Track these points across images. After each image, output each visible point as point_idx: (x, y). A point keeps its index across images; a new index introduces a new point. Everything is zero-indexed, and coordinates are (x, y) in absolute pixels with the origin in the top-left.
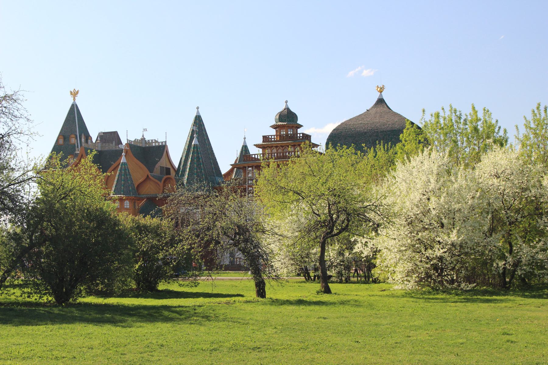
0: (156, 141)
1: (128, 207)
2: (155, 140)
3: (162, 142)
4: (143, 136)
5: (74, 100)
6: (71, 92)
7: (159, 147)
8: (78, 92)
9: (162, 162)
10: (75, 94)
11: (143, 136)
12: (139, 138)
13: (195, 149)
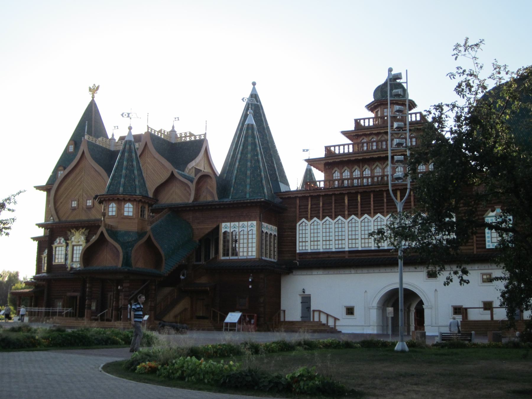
0: (191, 135)
1: (131, 214)
2: (190, 133)
3: (200, 135)
4: (173, 127)
5: (93, 97)
6: (90, 89)
7: (195, 141)
8: (98, 88)
9: (198, 163)
10: (94, 90)
11: (173, 127)
12: (168, 129)
13: (250, 131)
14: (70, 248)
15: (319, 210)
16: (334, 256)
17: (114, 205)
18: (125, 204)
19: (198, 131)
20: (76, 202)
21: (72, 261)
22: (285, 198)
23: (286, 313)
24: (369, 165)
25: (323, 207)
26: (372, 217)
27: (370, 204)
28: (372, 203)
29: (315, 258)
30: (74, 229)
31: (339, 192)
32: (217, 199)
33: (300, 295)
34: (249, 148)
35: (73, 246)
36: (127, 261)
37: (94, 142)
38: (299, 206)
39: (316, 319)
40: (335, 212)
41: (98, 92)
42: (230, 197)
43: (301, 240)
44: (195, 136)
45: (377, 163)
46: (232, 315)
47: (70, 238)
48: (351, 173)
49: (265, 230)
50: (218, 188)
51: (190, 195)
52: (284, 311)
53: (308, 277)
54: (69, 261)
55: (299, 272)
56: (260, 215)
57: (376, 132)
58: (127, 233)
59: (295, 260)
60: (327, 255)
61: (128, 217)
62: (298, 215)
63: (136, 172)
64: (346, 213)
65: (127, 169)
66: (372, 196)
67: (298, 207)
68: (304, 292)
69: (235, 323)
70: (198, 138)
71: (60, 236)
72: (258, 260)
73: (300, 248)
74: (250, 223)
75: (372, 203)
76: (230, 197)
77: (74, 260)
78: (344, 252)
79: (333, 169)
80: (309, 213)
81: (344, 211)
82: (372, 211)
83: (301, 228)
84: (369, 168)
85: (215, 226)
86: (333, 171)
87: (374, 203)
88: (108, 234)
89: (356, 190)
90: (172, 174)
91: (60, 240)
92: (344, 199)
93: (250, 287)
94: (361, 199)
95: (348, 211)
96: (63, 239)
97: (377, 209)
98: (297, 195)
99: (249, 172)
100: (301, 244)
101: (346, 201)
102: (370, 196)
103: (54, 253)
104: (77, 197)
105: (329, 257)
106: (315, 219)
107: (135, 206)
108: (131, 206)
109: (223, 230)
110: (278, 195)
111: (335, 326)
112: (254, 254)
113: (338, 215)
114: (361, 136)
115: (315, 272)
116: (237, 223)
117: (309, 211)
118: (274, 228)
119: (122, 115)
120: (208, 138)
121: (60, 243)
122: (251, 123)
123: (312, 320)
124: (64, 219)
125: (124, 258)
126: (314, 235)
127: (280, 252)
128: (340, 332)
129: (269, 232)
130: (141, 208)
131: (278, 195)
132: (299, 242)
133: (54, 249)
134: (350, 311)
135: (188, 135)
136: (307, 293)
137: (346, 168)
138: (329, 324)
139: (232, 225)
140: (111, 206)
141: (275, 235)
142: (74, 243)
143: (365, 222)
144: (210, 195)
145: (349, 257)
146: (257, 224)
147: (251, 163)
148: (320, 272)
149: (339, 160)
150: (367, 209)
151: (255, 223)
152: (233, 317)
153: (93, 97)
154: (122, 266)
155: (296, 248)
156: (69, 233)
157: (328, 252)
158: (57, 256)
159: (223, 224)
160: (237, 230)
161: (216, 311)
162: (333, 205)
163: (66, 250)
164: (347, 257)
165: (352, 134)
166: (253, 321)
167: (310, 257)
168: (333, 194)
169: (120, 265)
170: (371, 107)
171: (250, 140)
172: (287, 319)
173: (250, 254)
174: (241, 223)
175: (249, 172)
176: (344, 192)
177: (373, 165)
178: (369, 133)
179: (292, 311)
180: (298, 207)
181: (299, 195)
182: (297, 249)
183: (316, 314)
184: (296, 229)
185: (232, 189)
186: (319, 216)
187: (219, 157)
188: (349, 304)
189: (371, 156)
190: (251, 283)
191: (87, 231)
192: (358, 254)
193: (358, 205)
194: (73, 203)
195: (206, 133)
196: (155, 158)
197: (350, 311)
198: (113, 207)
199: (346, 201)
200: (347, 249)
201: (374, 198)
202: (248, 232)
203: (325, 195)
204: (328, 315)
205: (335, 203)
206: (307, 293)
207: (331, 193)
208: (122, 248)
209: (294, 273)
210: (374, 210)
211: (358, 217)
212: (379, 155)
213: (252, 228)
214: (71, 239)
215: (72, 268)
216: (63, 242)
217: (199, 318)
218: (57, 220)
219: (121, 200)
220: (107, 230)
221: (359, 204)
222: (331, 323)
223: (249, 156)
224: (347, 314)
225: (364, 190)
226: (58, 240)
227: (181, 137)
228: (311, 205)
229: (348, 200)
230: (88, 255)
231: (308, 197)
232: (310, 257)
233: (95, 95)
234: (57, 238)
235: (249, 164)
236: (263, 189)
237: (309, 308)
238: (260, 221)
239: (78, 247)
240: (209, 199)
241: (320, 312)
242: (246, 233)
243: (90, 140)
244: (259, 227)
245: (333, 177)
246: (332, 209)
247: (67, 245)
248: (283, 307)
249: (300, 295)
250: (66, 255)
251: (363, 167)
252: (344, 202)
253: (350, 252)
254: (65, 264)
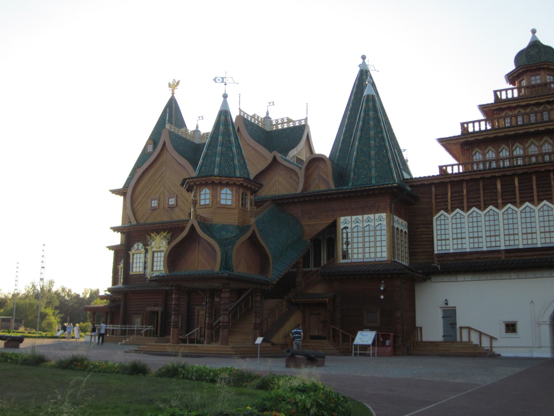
0: (289, 121)
1: (229, 202)
2: (288, 119)
3: (300, 121)
5: (173, 94)
7: (295, 128)
9: (298, 152)
10: (174, 85)
12: (263, 115)
13: (371, 104)
14: (149, 255)
15: (463, 199)
16: (486, 256)
17: (208, 191)
18: (221, 190)
19: (297, 116)
20: (156, 201)
21: (152, 270)
22: (417, 186)
23: (423, 329)
24: (521, 144)
25: (467, 195)
26: (536, 205)
27: (532, 189)
28: (535, 187)
29: (460, 260)
30: (155, 233)
31: (489, 175)
32: (333, 187)
33: (441, 307)
34: (372, 123)
35: (154, 252)
36: (226, 264)
37: (176, 132)
38: (436, 195)
39: (465, 339)
40: (484, 201)
41: (178, 87)
42: (351, 184)
43: (439, 238)
44: (294, 122)
45: (532, 140)
46: (363, 335)
47: (149, 243)
48: (498, 153)
49: (396, 225)
50: (333, 174)
51: (298, 184)
52: (421, 328)
53: (442, 284)
54: (148, 270)
55: (439, 279)
56: (391, 205)
57: (524, 103)
58: (225, 227)
59: (433, 263)
60: (475, 256)
61: (225, 207)
62: (434, 207)
63: (234, 149)
64: (500, 201)
65: (222, 145)
66: (534, 178)
67: (433, 197)
68: (447, 304)
69: (369, 346)
70: (297, 124)
71: (138, 241)
72: (390, 262)
73: (438, 248)
74: (377, 215)
75: (535, 187)
76: (351, 184)
77: (155, 269)
78: (499, 251)
79: (473, 151)
80: (449, 204)
81: (497, 200)
82: (535, 198)
83: (439, 223)
84: (521, 147)
85: (331, 221)
86: (474, 153)
87: (537, 188)
88: (201, 228)
89: (513, 172)
90: (275, 159)
91: (138, 245)
92: (496, 185)
93: (382, 297)
94: (519, 183)
95: (502, 200)
96: (141, 245)
97: (542, 195)
98: (432, 181)
99: (373, 152)
100: (439, 243)
101: (499, 187)
102: (532, 178)
103: (131, 261)
104: (157, 195)
105: (478, 258)
106: (458, 210)
107: (234, 192)
108: (229, 192)
109: (342, 226)
110: (406, 183)
111: (491, 347)
112: (385, 254)
113: (489, 205)
114: (504, 109)
115: (461, 278)
116: (360, 217)
117: (449, 201)
118: (405, 223)
119: (215, 80)
120: (309, 123)
121: (138, 249)
122: (372, 94)
123: (458, 340)
124: (142, 221)
125: (222, 260)
126: (456, 231)
127: (412, 254)
128: (499, 355)
129: (400, 228)
130: (243, 194)
131: (406, 183)
132: (438, 240)
133: (131, 256)
134: (511, 327)
135: (286, 121)
136: (450, 304)
137: (490, 147)
138: (483, 346)
139: (353, 220)
140: (203, 192)
141: (405, 232)
142: (154, 249)
143: (525, 212)
144: (324, 182)
145: (505, 257)
146: (387, 216)
147: (375, 141)
148: (469, 277)
149: (482, 137)
150: (529, 195)
151: (384, 215)
152: (365, 337)
153: (173, 94)
154: (220, 270)
155: (433, 248)
156: (149, 237)
157: (476, 252)
158: (135, 265)
159: (342, 219)
160: (361, 225)
161: (337, 329)
162: (482, 192)
163: (145, 258)
164: (503, 258)
165: (493, 108)
166: (388, 342)
167: (453, 258)
168: (481, 178)
169: (217, 269)
170: (512, 78)
171: (371, 113)
172: (424, 339)
173: (379, 255)
174: (365, 216)
175: (373, 152)
176: (497, 175)
177: (527, 142)
178: (515, 105)
179: (432, 329)
180: (433, 197)
181: (436, 181)
182: (435, 249)
183: (465, 332)
184: (432, 224)
185: (352, 174)
186: (463, 207)
187: (323, 142)
188: (510, 319)
189: (527, 130)
190: (383, 292)
191: (170, 234)
192: (519, 254)
193: (515, 191)
194: (153, 202)
195: (307, 118)
196: (249, 145)
197: (511, 327)
198: (205, 194)
199: (499, 187)
200: (503, 248)
201: (537, 181)
202: (375, 227)
203: (471, 179)
204: (481, 334)
205: (484, 190)
206: (450, 304)
207: (479, 177)
208: (220, 246)
209: (433, 279)
210: (538, 196)
211: (516, 206)
212: (536, 129)
213: (380, 222)
214: (151, 244)
216: (142, 247)
217: (313, 338)
218: (134, 222)
219: (217, 184)
220: (199, 223)
221: (517, 190)
222: (486, 343)
223: (372, 133)
224: (507, 332)
225: (525, 170)
226: (135, 246)
227: (277, 124)
228: (451, 194)
229: (501, 185)
230: (174, 258)
231: (447, 182)
232: (453, 258)
233: (175, 91)
234: (134, 243)
235: (372, 142)
236: (392, 173)
237: (453, 324)
238: (391, 212)
239: (159, 254)
240: (323, 187)
241: (469, 329)
242: (372, 228)
243: (172, 130)
244: (390, 222)
245: (473, 159)
246: (479, 197)
247: (146, 251)
248: (418, 324)
249: (441, 307)
250: (145, 263)
251: (513, 146)
252: (496, 188)
253: (507, 251)
254: (144, 274)
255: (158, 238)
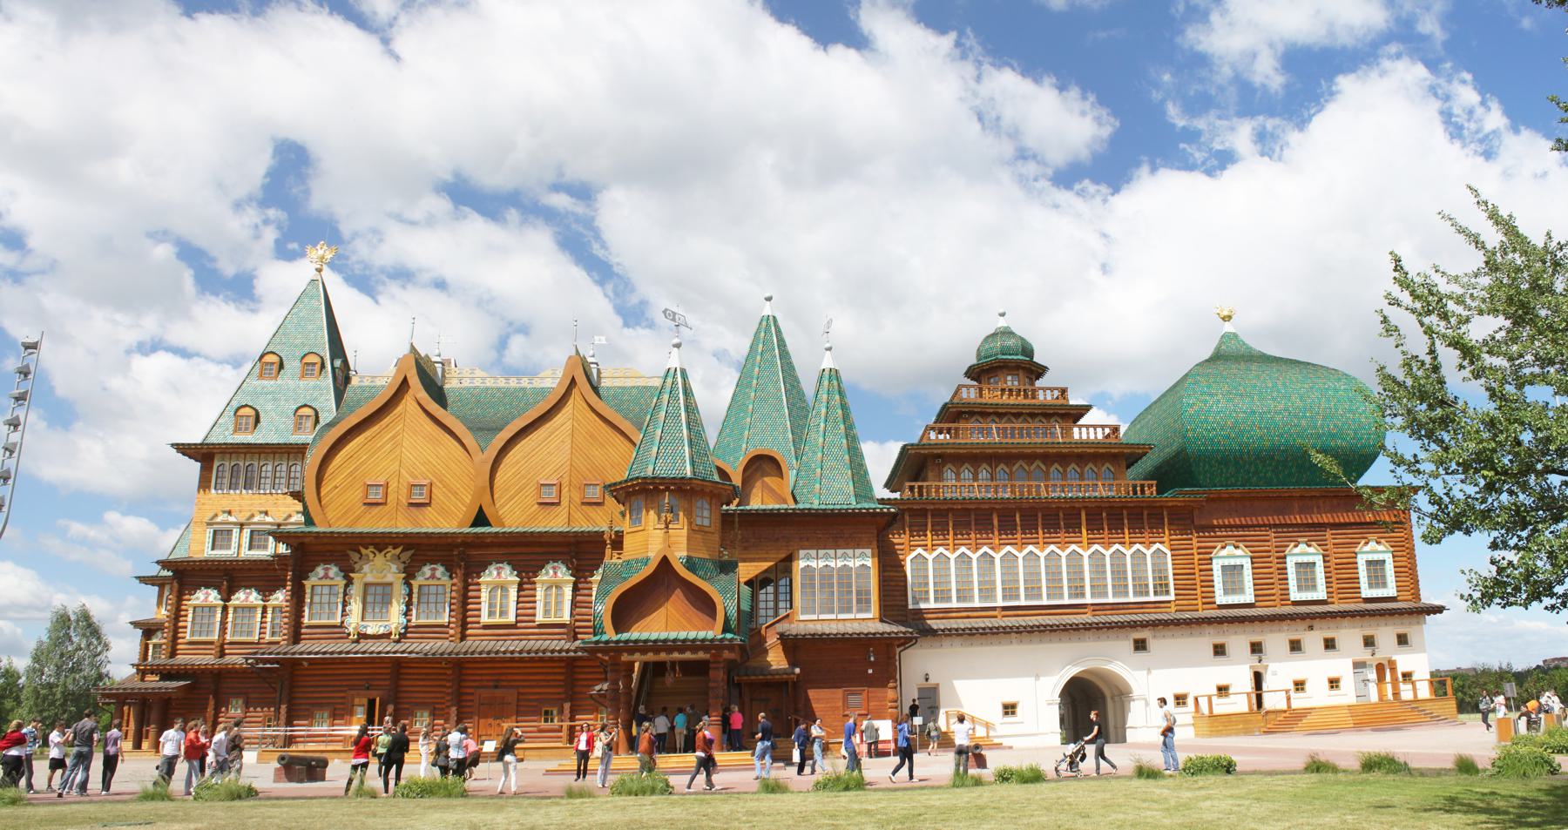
30: (371, 549)
35: (367, 585)
47: (357, 567)
78: (994, 609)
96: (334, 570)
101: (996, 522)
133: (308, 591)
136: (932, 681)
142: (370, 578)
156: (355, 556)
163: (345, 594)
191: (410, 553)
200: (1000, 603)
206: (932, 681)
215: (363, 636)
226: (320, 570)
255: (380, 558)
